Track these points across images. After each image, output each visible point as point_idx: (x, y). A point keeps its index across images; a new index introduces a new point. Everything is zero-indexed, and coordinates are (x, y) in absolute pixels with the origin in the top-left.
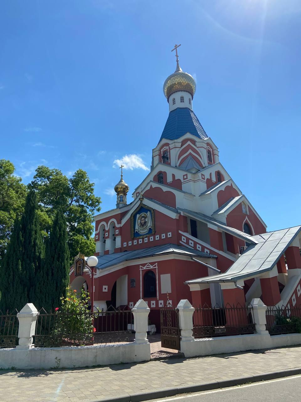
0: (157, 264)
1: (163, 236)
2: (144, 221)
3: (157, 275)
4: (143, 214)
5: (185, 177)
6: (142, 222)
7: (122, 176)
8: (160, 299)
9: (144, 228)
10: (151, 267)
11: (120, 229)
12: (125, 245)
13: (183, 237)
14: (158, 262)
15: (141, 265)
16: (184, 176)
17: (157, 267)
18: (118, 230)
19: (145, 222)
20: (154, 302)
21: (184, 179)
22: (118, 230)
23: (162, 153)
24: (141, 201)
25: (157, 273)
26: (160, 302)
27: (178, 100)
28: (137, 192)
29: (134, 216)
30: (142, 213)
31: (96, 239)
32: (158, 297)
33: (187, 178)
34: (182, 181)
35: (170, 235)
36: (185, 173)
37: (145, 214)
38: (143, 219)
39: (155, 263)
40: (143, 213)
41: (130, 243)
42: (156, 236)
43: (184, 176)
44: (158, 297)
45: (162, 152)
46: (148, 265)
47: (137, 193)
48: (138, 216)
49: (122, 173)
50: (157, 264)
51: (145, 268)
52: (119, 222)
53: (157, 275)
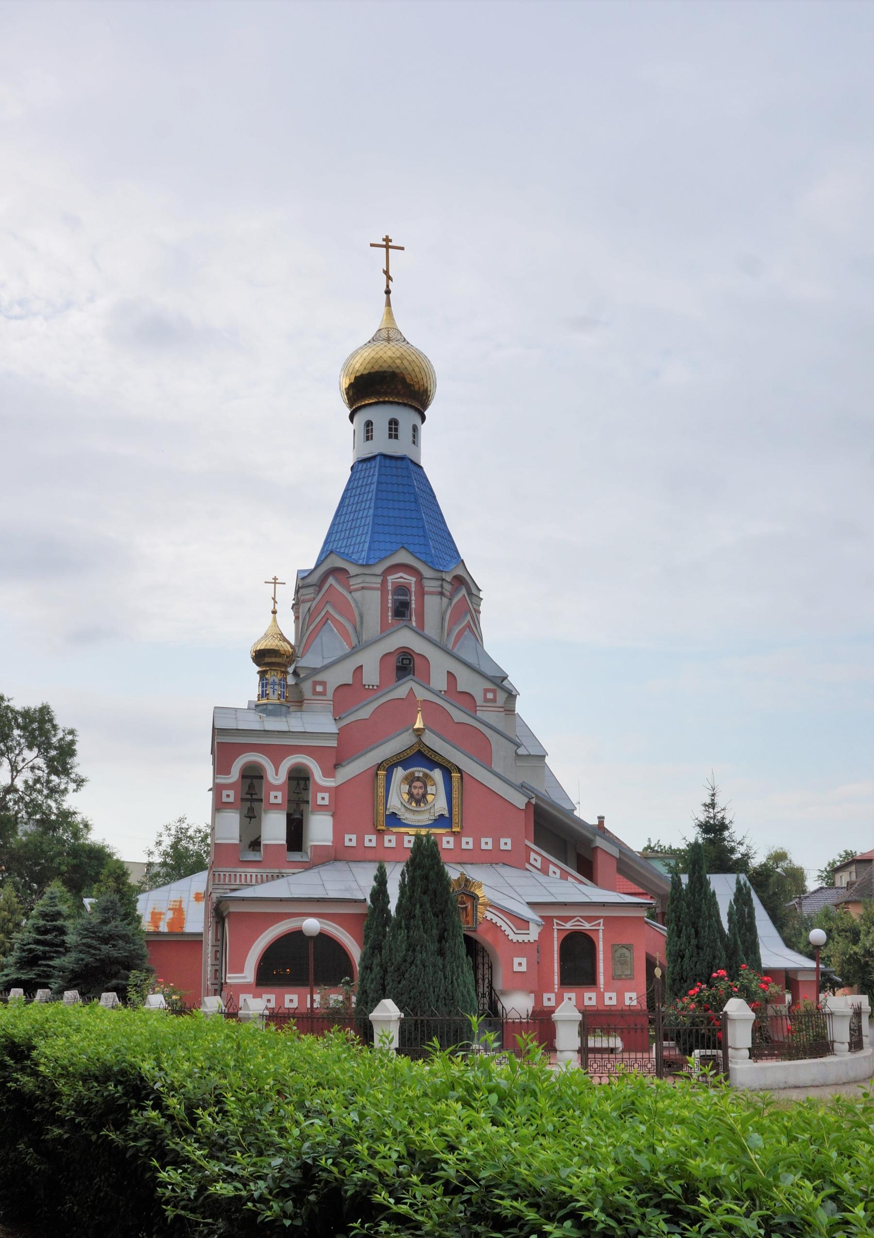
0: (601, 921)
1: (487, 843)
2: (421, 791)
3: (601, 943)
4: (419, 771)
5: (490, 696)
6: (415, 791)
7: (274, 612)
8: (606, 990)
9: (409, 807)
10: (587, 926)
11: (336, 792)
12: (351, 840)
13: (533, 855)
14: (605, 918)
15: (558, 918)
16: (486, 691)
17: (602, 927)
18: (326, 796)
19: (424, 796)
20: (593, 995)
21: (486, 700)
22: (326, 796)
23: (390, 588)
24: (419, 736)
25: (601, 940)
26: (607, 995)
27: (404, 430)
28: (319, 678)
29: (389, 766)
30: (418, 769)
31: (225, 799)
32: (602, 986)
33: (494, 700)
34: (479, 701)
35: (506, 844)
36: (492, 686)
37: (426, 775)
38: (418, 784)
39: (598, 918)
40: (421, 769)
41: (370, 840)
42: (464, 840)
43: (486, 691)
44: (602, 986)
45: (390, 584)
46: (578, 921)
47: (315, 683)
48: (399, 773)
49: (275, 602)
50: (601, 921)
51: (568, 926)
52: (329, 773)
53: (601, 943)
